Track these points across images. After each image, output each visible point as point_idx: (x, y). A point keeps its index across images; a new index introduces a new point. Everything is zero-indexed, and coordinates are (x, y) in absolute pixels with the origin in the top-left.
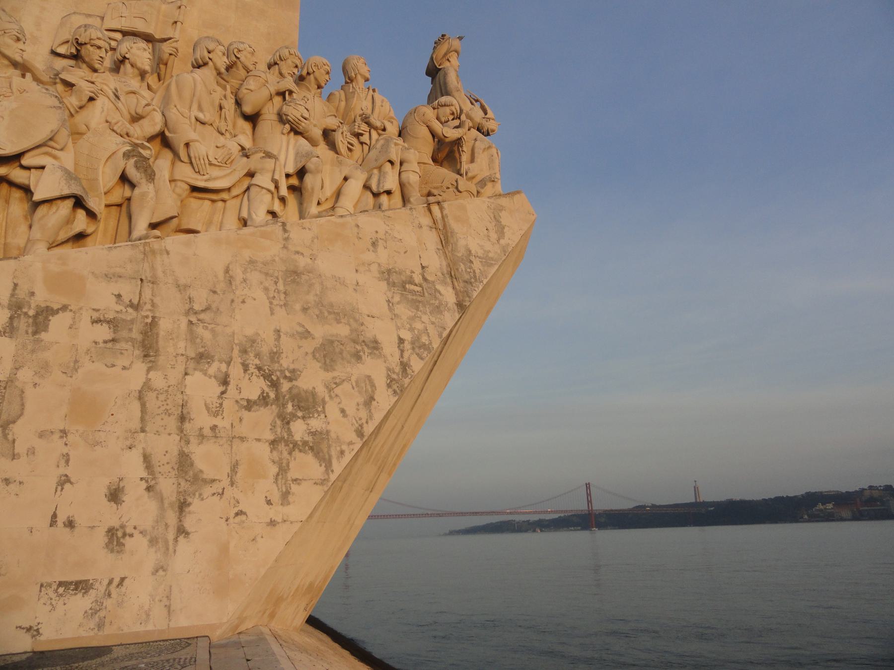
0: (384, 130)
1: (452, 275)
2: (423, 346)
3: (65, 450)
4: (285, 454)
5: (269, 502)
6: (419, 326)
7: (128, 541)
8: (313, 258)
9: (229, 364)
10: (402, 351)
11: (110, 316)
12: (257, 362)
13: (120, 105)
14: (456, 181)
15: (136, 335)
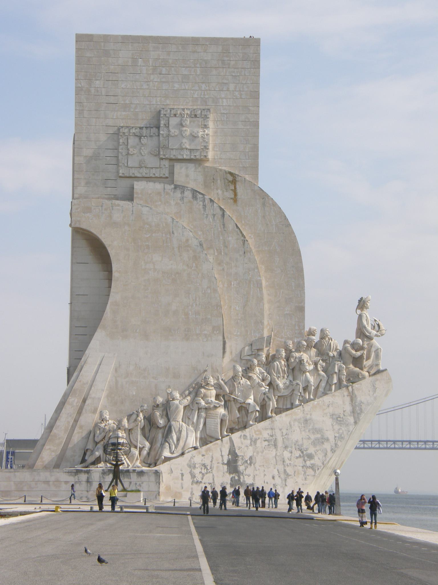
0: (334, 356)
1: (353, 412)
2: (342, 438)
3: (264, 469)
4: (305, 469)
5: (302, 480)
6: (341, 431)
7: (276, 486)
8: (311, 415)
9: (292, 448)
10: (335, 440)
11: (267, 439)
12: (298, 447)
13: (261, 378)
14: (359, 374)
15: (273, 443)
